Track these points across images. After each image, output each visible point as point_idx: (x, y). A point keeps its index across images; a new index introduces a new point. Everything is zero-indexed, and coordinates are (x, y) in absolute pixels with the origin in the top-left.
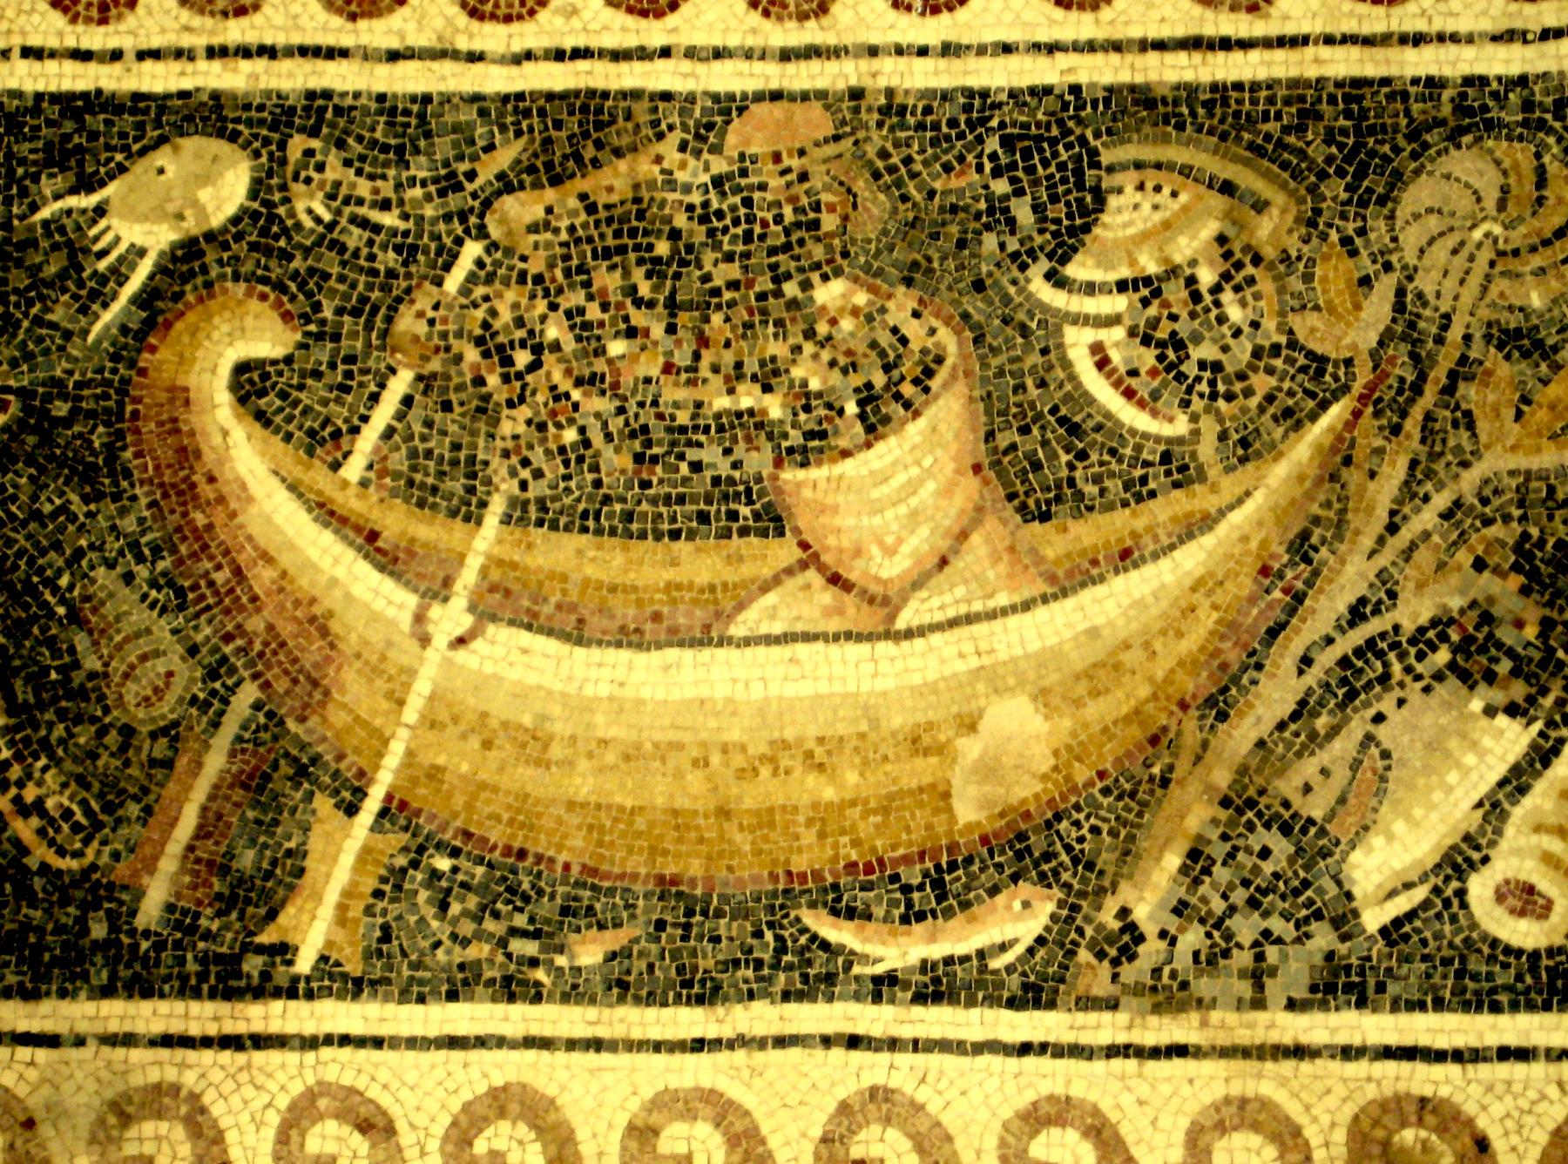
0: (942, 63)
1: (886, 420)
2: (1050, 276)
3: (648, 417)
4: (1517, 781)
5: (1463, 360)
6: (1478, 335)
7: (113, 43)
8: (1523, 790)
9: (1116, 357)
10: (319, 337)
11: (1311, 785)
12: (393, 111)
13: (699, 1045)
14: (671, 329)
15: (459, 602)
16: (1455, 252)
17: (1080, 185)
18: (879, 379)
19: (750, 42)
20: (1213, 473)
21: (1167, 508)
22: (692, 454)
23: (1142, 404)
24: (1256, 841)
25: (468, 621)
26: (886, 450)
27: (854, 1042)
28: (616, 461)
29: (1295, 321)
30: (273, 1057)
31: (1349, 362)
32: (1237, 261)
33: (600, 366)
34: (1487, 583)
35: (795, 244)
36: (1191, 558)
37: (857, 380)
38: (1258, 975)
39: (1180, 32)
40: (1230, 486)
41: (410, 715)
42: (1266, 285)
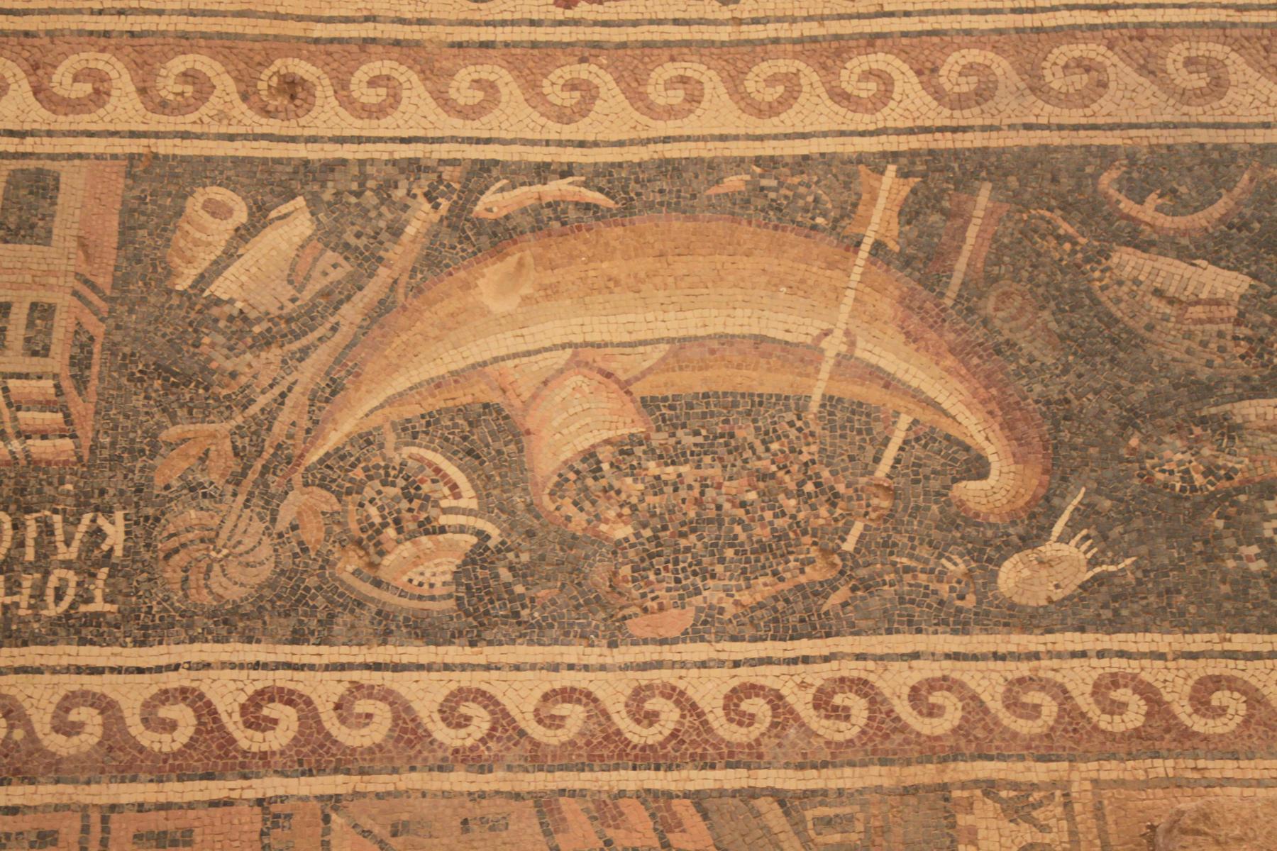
0: (558, 660)
1: (584, 460)
2: (488, 537)
4: (218, 267)
5: (238, 484)
6: (228, 497)
7: (1105, 662)
8: (215, 262)
9: (446, 491)
10: (938, 494)
11: (332, 269)
12: (910, 623)
13: (666, 140)
14: (719, 507)
15: (830, 353)
16: (239, 542)
17: (468, 587)
18: (590, 482)
19: (683, 672)
20: (387, 426)
21: (411, 410)
22: (699, 440)
23: (430, 464)
25: (824, 344)
26: (584, 443)
27: (582, 144)
28: (745, 432)
29: (337, 507)
30: (900, 124)
31: (306, 485)
33: (761, 485)
34: (229, 365)
36: (400, 383)
37: (603, 482)
39: (406, 674)
40: (376, 420)
41: (851, 294)
42: (354, 526)
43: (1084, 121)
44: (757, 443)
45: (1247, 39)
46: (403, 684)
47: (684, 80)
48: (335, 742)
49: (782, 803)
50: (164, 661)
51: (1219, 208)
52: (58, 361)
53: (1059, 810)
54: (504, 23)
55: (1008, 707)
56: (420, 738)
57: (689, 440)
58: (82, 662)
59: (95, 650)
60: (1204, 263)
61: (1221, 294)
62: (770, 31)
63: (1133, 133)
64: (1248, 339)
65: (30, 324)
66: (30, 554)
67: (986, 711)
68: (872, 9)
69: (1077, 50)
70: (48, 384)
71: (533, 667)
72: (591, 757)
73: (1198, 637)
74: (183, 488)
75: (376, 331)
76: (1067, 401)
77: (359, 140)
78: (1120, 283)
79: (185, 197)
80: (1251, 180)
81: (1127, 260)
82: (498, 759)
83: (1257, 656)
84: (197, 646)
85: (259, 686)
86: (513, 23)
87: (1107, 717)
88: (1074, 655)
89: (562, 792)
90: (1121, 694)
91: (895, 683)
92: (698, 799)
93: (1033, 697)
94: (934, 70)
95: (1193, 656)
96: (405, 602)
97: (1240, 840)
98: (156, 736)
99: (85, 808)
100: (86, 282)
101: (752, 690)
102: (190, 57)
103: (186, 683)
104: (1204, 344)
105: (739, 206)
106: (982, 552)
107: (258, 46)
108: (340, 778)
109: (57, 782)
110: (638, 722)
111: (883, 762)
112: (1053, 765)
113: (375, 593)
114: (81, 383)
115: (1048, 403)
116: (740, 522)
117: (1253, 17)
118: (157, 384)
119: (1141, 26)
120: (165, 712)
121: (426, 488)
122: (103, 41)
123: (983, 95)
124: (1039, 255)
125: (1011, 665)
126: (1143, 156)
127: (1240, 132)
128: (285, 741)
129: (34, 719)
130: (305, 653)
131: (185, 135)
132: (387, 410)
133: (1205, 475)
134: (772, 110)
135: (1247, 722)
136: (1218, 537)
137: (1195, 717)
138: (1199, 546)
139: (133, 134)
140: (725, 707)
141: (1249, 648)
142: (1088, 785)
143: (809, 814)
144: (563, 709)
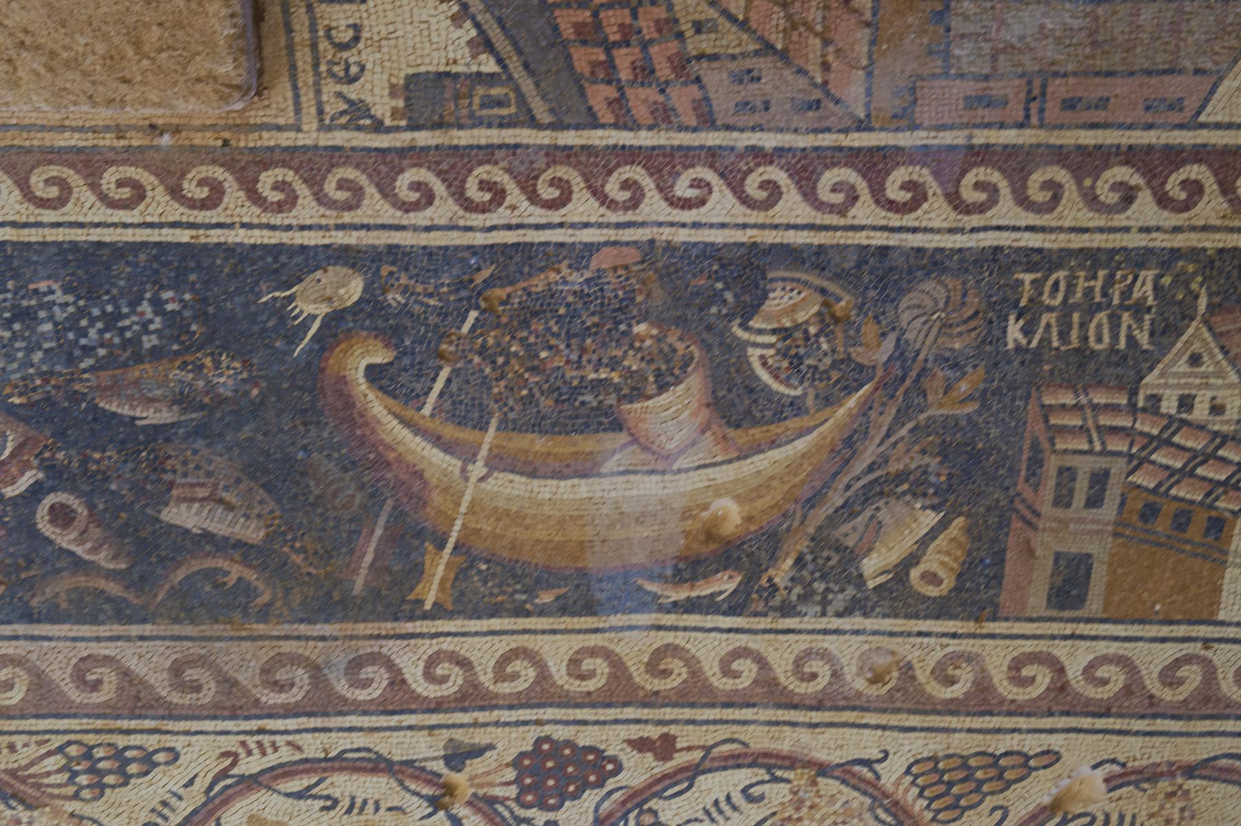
0: (693, 231)
2: (741, 325)
3: (559, 383)
4: (933, 534)
5: (924, 369)
6: (931, 358)
7: (287, 222)
8: (934, 538)
9: (770, 361)
10: (405, 354)
12: (431, 254)
13: (596, 631)
14: (568, 346)
15: (480, 463)
17: (757, 286)
18: (664, 367)
21: (793, 423)
22: (581, 398)
23: (781, 382)
24: (825, 554)
26: (665, 398)
27: (659, 628)
28: (546, 403)
30: (420, 641)
31: (874, 367)
32: (829, 320)
33: (536, 363)
34: (927, 459)
35: (623, 310)
36: (801, 445)
37: (653, 367)
38: (825, 603)
39: (805, 221)
40: (820, 416)
41: (463, 509)
42: (840, 335)
43: (281, 643)
44: (538, 395)
45: (152, 707)
47: (582, 677)
48: (859, 171)
49: (533, 118)
50: (981, 235)
51: (180, 575)
52: (1052, 464)
53: (327, 109)
54: (715, 722)
55: (361, 188)
56: (797, 173)
57: (588, 398)
58: (1040, 236)
59: (1031, 244)
60: (195, 530)
61: (184, 507)
62: (513, 716)
63: (244, 633)
64: (164, 471)
65: (1071, 491)
66: (1076, 317)
67: (377, 185)
68: (437, 732)
69: (281, 698)
70: (1060, 446)
71: (711, 226)
72: (672, 155)
73: (215, 240)
74: (965, 366)
75: (818, 484)
76: (305, 424)
77: (825, 632)
78: (259, 516)
79: (955, 589)
80: (155, 596)
81: (253, 533)
82: (741, 156)
83: (174, 225)
84: (958, 246)
85: (913, 215)
86: (707, 722)
87: (289, 179)
88: (309, 228)
89: (695, 130)
90: (275, 197)
91: (444, 209)
92: (595, 124)
93: (341, 196)
94: (392, 684)
95: (219, 226)
96: (805, 277)
97: (199, 80)
98: (989, 178)
99: (1041, 126)
100: (1030, 524)
101: (552, 205)
102: (948, 696)
103: (966, 218)
104: (198, 467)
106: (374, 308)
107: (898, 705)
108: (856, 144)
109: (1061, 146)
110: (635, 182)
111: (456, 147)
112: (330, 143)
113: (825, 284)
114: (1036, 447)
115: (318, 423)
116: (553, 335)
117: (148, 724)
118: (980, 445)
119: (233, 717)
120: (982, 197)
121: (785, 364)
122: (1013, 708)
123: (356, 665)
124: (320, 539)
125: (356, 221)
126: (237, 616)
127: (162, 634)
128: (895, 173)
129: (1075, 194)
130: (879, 239)
131: (954, 636)
132: (812, 424)
133: (202, 366)
134: (514, 654)
135: (183, 175)
136: (195, 318)
137: (221, 178)
138: (211, 310)
139: (992, 636)
140: (571, 192)
141: (178, 231)
142: (305, 128)
143: (513, 110)
144: (691, 193)
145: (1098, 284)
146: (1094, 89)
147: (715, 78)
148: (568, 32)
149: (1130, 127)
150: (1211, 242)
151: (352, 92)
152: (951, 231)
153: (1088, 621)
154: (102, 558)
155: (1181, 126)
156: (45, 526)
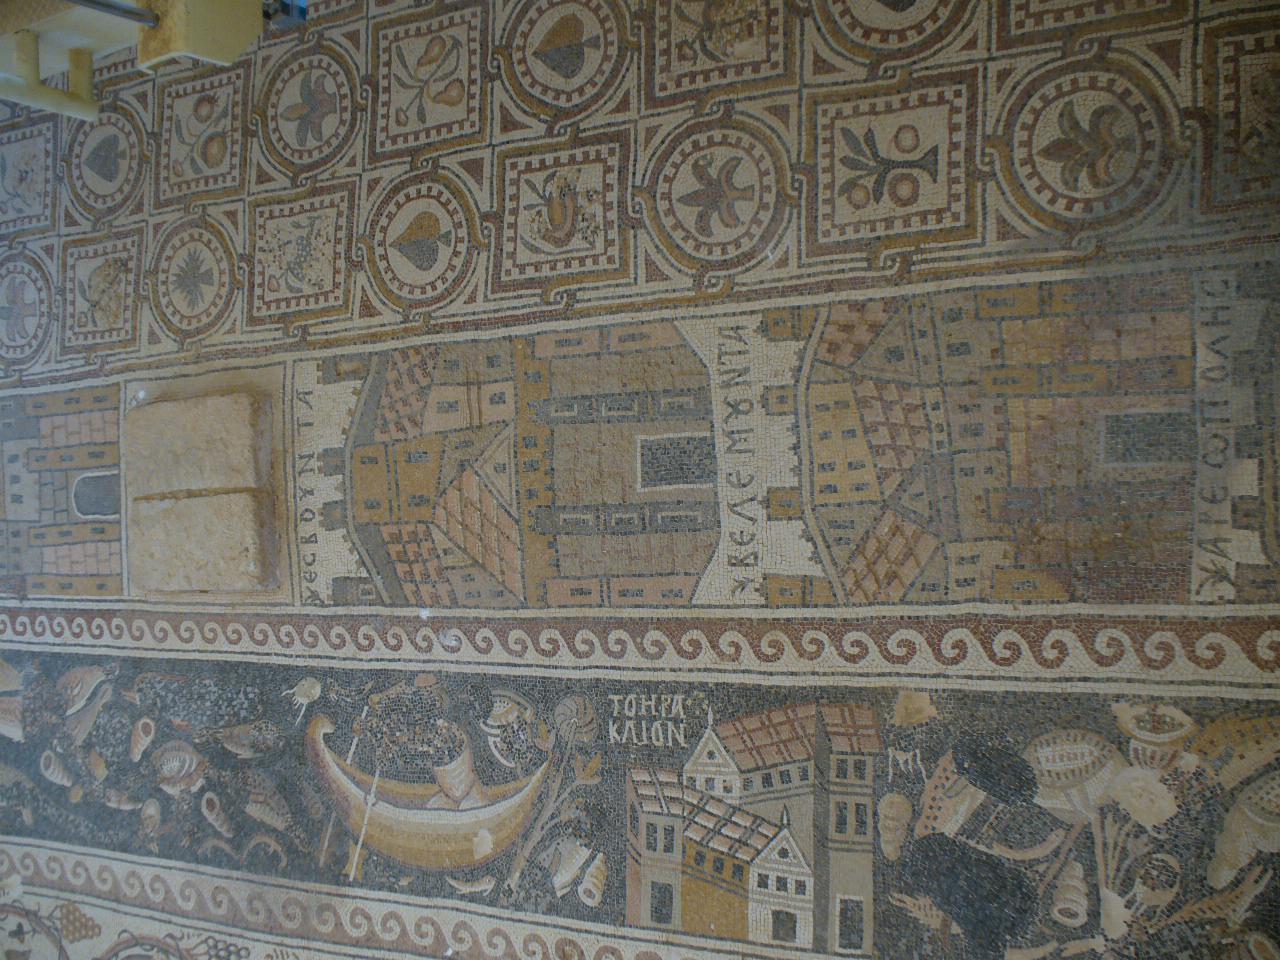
11: (544, 858)
13: (427, 907)
21: (512, 785)
28: (400, 762)
32: (522, 723)
35: (430, 712)
36: (517, 798)
38: (536, 904)
46: (505, 657)
52: (643, 820)
77: (538, 924)
81: (280, 824)
91: (349, 650)
93: (310, 640)
105: (402, 872)
119: (271, 933)
145: (653, 703)
146: (633, 585)
147: (455, 577)
148: (394, 556)
149: (657, 607)
150: (712, 679)
151: (313, 586)
152: (574, 668)
153: (675, 932)
154: (223, 830)
155: (683, 607)
156: (205, 811)
